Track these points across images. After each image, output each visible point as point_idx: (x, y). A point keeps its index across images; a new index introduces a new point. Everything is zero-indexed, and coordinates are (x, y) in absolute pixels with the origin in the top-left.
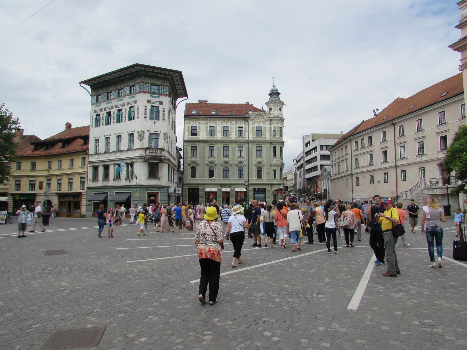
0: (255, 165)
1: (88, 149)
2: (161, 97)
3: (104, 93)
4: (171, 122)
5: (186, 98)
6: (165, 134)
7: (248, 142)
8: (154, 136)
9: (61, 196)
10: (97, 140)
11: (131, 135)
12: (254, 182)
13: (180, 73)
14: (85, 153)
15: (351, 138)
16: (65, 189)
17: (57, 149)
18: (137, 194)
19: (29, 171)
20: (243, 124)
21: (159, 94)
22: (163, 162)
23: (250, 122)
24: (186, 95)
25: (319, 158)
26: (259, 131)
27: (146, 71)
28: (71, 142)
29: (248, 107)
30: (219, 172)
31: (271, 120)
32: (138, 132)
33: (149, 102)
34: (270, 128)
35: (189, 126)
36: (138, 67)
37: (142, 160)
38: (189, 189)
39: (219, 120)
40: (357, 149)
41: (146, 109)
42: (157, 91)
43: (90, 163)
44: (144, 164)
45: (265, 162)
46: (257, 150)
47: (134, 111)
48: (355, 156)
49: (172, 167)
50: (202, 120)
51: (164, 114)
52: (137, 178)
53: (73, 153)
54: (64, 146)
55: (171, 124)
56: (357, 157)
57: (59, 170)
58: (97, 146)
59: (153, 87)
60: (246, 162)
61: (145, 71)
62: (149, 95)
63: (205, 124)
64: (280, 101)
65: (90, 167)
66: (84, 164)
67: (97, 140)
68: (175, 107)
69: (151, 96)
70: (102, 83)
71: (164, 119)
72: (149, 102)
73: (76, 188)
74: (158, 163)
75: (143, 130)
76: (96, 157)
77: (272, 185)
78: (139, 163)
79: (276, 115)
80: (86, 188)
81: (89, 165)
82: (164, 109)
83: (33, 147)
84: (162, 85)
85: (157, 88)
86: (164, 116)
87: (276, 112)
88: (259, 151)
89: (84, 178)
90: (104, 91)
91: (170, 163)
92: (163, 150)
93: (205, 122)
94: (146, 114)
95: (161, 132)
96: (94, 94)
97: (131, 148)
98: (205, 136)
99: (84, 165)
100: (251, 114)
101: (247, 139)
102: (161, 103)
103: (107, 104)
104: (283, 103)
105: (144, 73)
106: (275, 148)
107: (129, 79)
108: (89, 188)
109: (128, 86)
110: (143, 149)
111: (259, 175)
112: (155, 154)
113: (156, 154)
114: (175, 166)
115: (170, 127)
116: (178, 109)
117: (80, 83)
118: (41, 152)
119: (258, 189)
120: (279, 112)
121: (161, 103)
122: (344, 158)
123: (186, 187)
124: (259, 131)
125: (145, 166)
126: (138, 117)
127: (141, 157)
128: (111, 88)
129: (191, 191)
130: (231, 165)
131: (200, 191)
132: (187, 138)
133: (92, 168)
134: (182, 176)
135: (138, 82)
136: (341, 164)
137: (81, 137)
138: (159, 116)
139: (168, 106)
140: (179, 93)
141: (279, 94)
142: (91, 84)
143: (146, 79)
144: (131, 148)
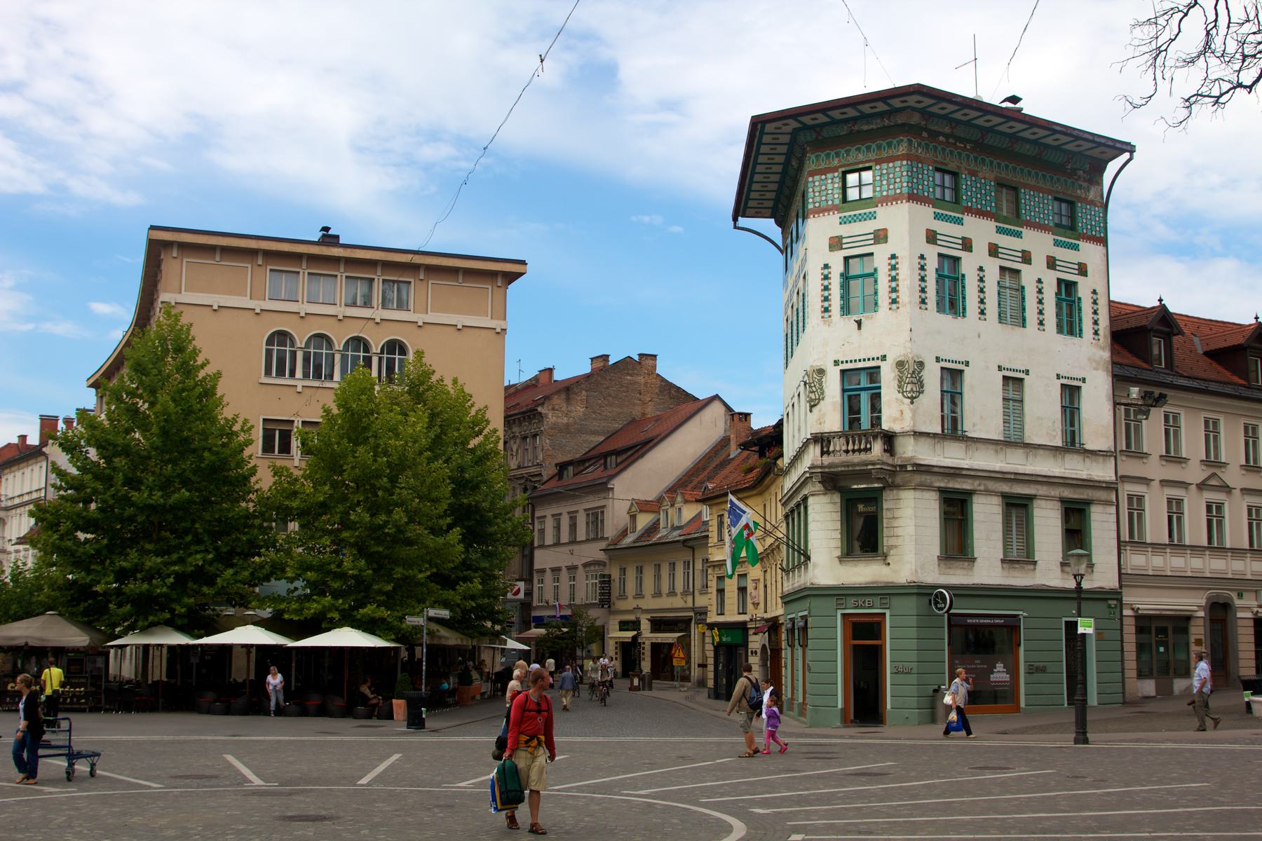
2: (881, 211)
5: (1126, 156)
6: (900, 364)
22: (897, 487)
41: (826, 277)
59: (852, 179)
62: (834, 218)
69: (843, 222)
71: (894, 301)
72: (836, 243)
75: (818, 364)
82: (893, 257)
85: (867, 176)
91: (966, 485)
94: (826, 299)
95: (884, 358)
102: (880, 237)
112: (844, 458)
125: (829, 507)
143: (823, 155)
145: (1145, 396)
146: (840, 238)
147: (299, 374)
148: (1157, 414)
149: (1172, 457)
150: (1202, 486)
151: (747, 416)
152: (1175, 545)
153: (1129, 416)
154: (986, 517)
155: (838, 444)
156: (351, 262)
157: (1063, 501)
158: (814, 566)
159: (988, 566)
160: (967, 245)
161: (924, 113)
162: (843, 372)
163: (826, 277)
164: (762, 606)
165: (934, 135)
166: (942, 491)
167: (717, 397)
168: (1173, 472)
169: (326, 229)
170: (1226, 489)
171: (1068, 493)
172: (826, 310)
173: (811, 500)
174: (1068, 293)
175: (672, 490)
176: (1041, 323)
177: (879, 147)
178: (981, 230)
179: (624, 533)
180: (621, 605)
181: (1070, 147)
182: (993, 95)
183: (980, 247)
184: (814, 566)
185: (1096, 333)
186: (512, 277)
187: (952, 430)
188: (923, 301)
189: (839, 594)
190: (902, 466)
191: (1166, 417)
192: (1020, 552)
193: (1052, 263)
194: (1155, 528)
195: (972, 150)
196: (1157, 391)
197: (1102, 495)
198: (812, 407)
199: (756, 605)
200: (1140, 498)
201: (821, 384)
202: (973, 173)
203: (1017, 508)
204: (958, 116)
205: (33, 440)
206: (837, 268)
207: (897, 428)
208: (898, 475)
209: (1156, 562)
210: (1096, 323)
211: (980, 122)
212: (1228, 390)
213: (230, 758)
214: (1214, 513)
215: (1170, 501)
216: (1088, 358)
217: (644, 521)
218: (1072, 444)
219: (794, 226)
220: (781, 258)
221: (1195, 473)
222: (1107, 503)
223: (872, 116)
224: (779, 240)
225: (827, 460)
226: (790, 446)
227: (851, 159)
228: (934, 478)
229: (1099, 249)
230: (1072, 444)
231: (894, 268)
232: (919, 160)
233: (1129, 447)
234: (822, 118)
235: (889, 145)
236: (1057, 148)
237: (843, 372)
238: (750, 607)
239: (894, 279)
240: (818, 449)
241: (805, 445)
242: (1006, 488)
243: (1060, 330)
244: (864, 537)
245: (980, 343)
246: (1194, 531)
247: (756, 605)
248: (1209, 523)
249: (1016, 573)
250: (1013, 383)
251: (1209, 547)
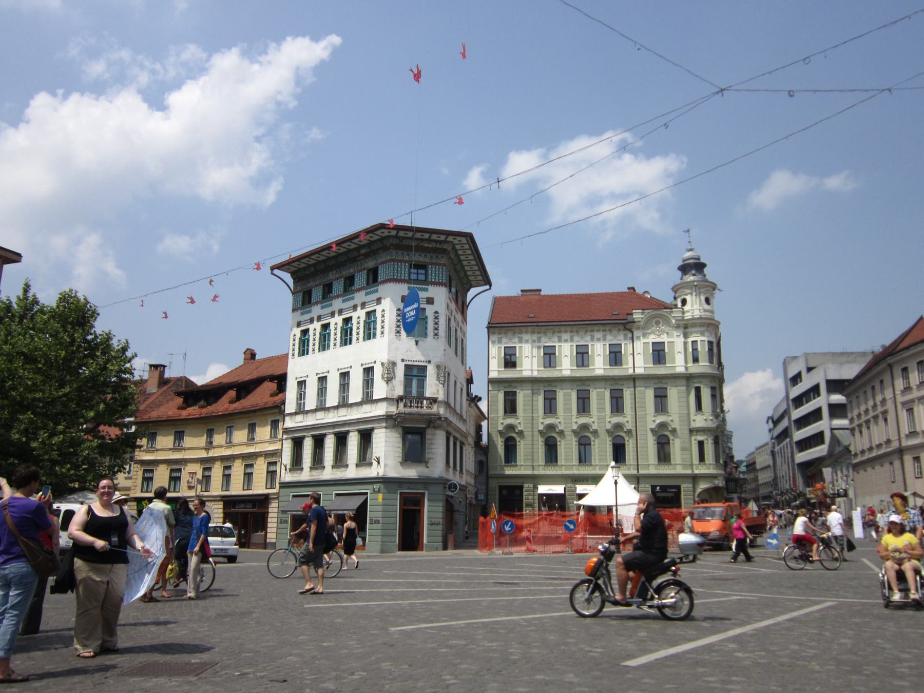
0: (652, 430)
1: (284, 403)
2: (430, 288)
3: (317, 286)
4: (453, 339)
5: (488, 287)
6: (438, 367)
7: (634, 379)
8: (415, 373)
9: (229, 502)
10: (302, 384)
11: (368, 371)
12: (653, 471)
13: (469, 237)
14: (277, 410)
15: (890, 360)
16: (237, 489)
17: (223, 405)
18: (380, 496)
19: (171, 449)
20: (621, 337)
22: (435, 428)
23: (637, 333)
24: (487, 281)
25: (825, 413)
26: (659, 354)
28: (253, 392)
29: (633, 298)
30: (567, 448)
31: (686, 327)
32: (382, 364)
34: (685, 343)
36: (383, 230)
37: (391, 422)
38: (501, 488)
39: (566, 332)
40: (908, 389)
42: (422, 277)
43: (286, 431)
45: (676, 425)
46: (656, 397)
47: (375, 322)
48: (903, 404)
49: (455, 439)
50: (526, 332)
51: (436, 323)
52: (379, 463)
53: (255, 411)
54: (239, 398)
55: (453, 344)
56: (909, 406)
57: (227, 447)
58: (301, 396)
60: (630, 426)
61: (396, 237)
63: (534, 341)
64: (707, 281)
65: (286, 439)
66: (274, 435)
67: (302, 384)
68: (463, 307)
70: (314, 265)
71: (436, 335)
73: (259, 487)
74: (425, 429)
75: (393, 359)
76: (299, 418)
77: (695, 478)
78: (384, 430)
79: (697, 314)
80: (278, 486)
81: (285, 437)
82: (436, 312)
83: (180, 400)
84: (432, 264)
86: (436, 329)
87: (697, 306)
88: (661, 398)
89: (275, 463)
90: (318, 282)
91: (450, 430)
92: (434, 400)
93: (535, 337)
96: (299, 288)
97: (368, 399)
98: (535, 367)
99: (276, 436)
100: (637, 315)
101: (631, 371)
102: (430, 301)
103: (322, 308)
104: (714, 287)
105: (395, 242)
106: (698, 390)
107: (367, 256)
108: (284, 485)
109: (364, 269)
110: (393, 399)
111: (664, 456)
113: (419, 410)
114: (465, 436)
115: (451, 352)
116: (470, 312)
117: (272, 268)
118: (193, 411)
119: (661, 487)
120: (707, 307)
121: (430, 301)
122: (880, 409)
123: (494, 484)
124: (659, 354)
126: (382, 333)
127: (388, 418)
128: (332, 276)
129: (505, 492)
130: (595, 432)
131: (525, 493)
132: (494, 375)
133: (290, 441)
134: (484, 460)
135: (383, 259)
136: (872, 425)
137: (272, 378)
138: (426, 328)
139: (444, 306)
140: (471, 278)
141: (704, 265)
142: (293, 269)
143: (400, 253)
144: (368, 399)
177: (431, 257)
213: (865, 560)
224: (292, 286)
231: (436, 318)
235: (437, 257)
239: (436, 323)
240: (401, 405)
244: (414, 451)
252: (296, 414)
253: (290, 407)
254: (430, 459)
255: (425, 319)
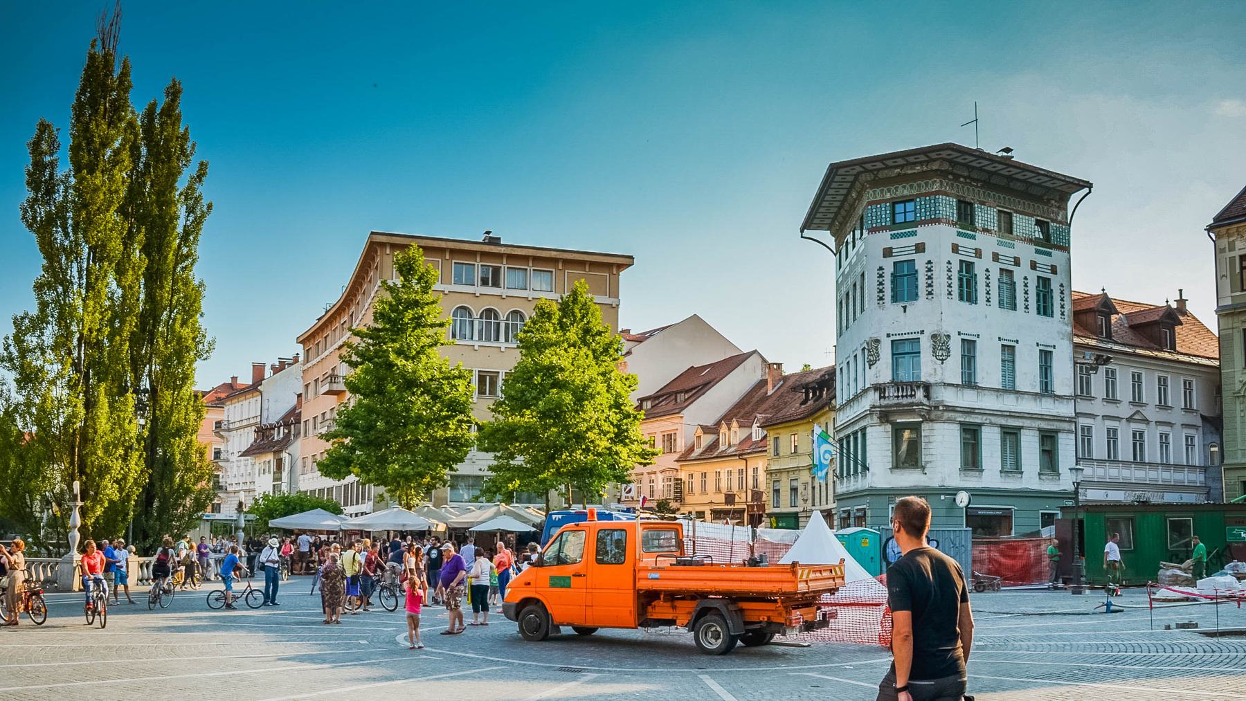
2: (919, 229)
5: (1086, 190)
6: (934, 337)
8: (904, 349)
21: (915, 223)
22: (932, 421)
27: (871, 171)
33: (888, 253)
35: (1232, 259)
41: (881, 276)
44: (881, 428)
51: (930, 278)
62: (888, 234)
69: (893, 237)
75: (875, 336)
82: (929, 262)
85: (910, 206)
86: (930, 285)
95: (922, 332)
97: (865, 391)
102: (920, 248)
105: (869, 177)
108: (839, 498)
112: (896, 401)
113: (901, 400)
145: (1098, 358)
146: (891, 249)
147: (476, 337)
148: (1102, 369)
149: (1111, 399)
150: (1130, 419)
151: (779, 365)
152: (1112, 460)
153: (1083, 372)
154: (991, 440)
155: (891, 392)
156: (510, 257)
157: (1040, 430)
158: (873, 474)
159: (991, 476)
160: (978, 253)
161: (952, 162)
162: (892, 341)
163: (881, 276)
164: (810, 501)
165: (957, 177)
166: (961, 423)
167: (755, 351)
168: (1111, 410)
169: (488, 233)
170: (1146, 421)
171: (1044, 425)
172: (881, 299)
173: (868, 430)
174: (1044, 287)
175: (727, 418)
176: (1027, 307)
177: (919, 186)
178: (988, 243)
179: (691, 449)
180: (688, 499)
181: (1048, 184)
182: (993, 149)
183: (987, 255)
184: (873, 474)
185: (1063, 314)
186: (621, 267)
187: (969, 382)
188: (950, 294)
189: (891, 493)
190: (936, 408)
191: (1107, 372)
192: (1013, 466)
193: (1034, 266)
194: (1099, 448)
195: (982, 187)
196: (1105, 355)
197: (1065, 426)
198: (870, 366)
199: (805, 501)
200: (1089, 428)
201: (877, 349)
202: (983, 203)
203: (1011, 435)
204: (974, 164)
205: (246, 379)
206: (889, 270)
207: (932, 381)
208: (935, 412)
209: (1099, 472)
210: (1062, 307)
211: (989, 168)
212: (1148, 353)
214: (1138, 437)
215: (1109, 430)
216: (1056, 332)
217: (707, 440)
218: (1046, 390)
219: (850, 238)
220: (833, 260)
221: (1125, 410)
222: (1069, 431)
223: (915, 164)
225: (884, 402)
226: (843, 391)
227: (899, 194)
228: (957, 415)
229: (1066, 254)
230: (1046, 390)
231: (929, 270)
232: (947, 195)
233: (1083, 392)
234: (879, 165)
235: (927, 184)
236: (1039, 185)
237: (892, 341)
238: (800, 502)
239: (930, 278)
240: (877, 394)
241: (865, 391)
242: (1003, 421)
243: (1039, 313)
244: (909, 455)
245: (986, 322)
246: (1152, 452)
247: (805, 501)
248: (1135, 445)
249: (1008, 480)
250: (1009, 350)
251: (1135, 462)
252: (840, 409)
253: (838, 402)
254: (927, 462)
255: (914, 274)
